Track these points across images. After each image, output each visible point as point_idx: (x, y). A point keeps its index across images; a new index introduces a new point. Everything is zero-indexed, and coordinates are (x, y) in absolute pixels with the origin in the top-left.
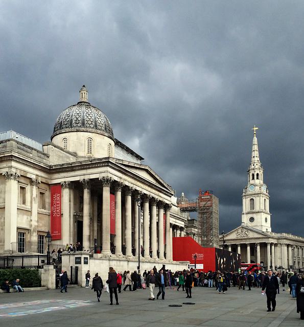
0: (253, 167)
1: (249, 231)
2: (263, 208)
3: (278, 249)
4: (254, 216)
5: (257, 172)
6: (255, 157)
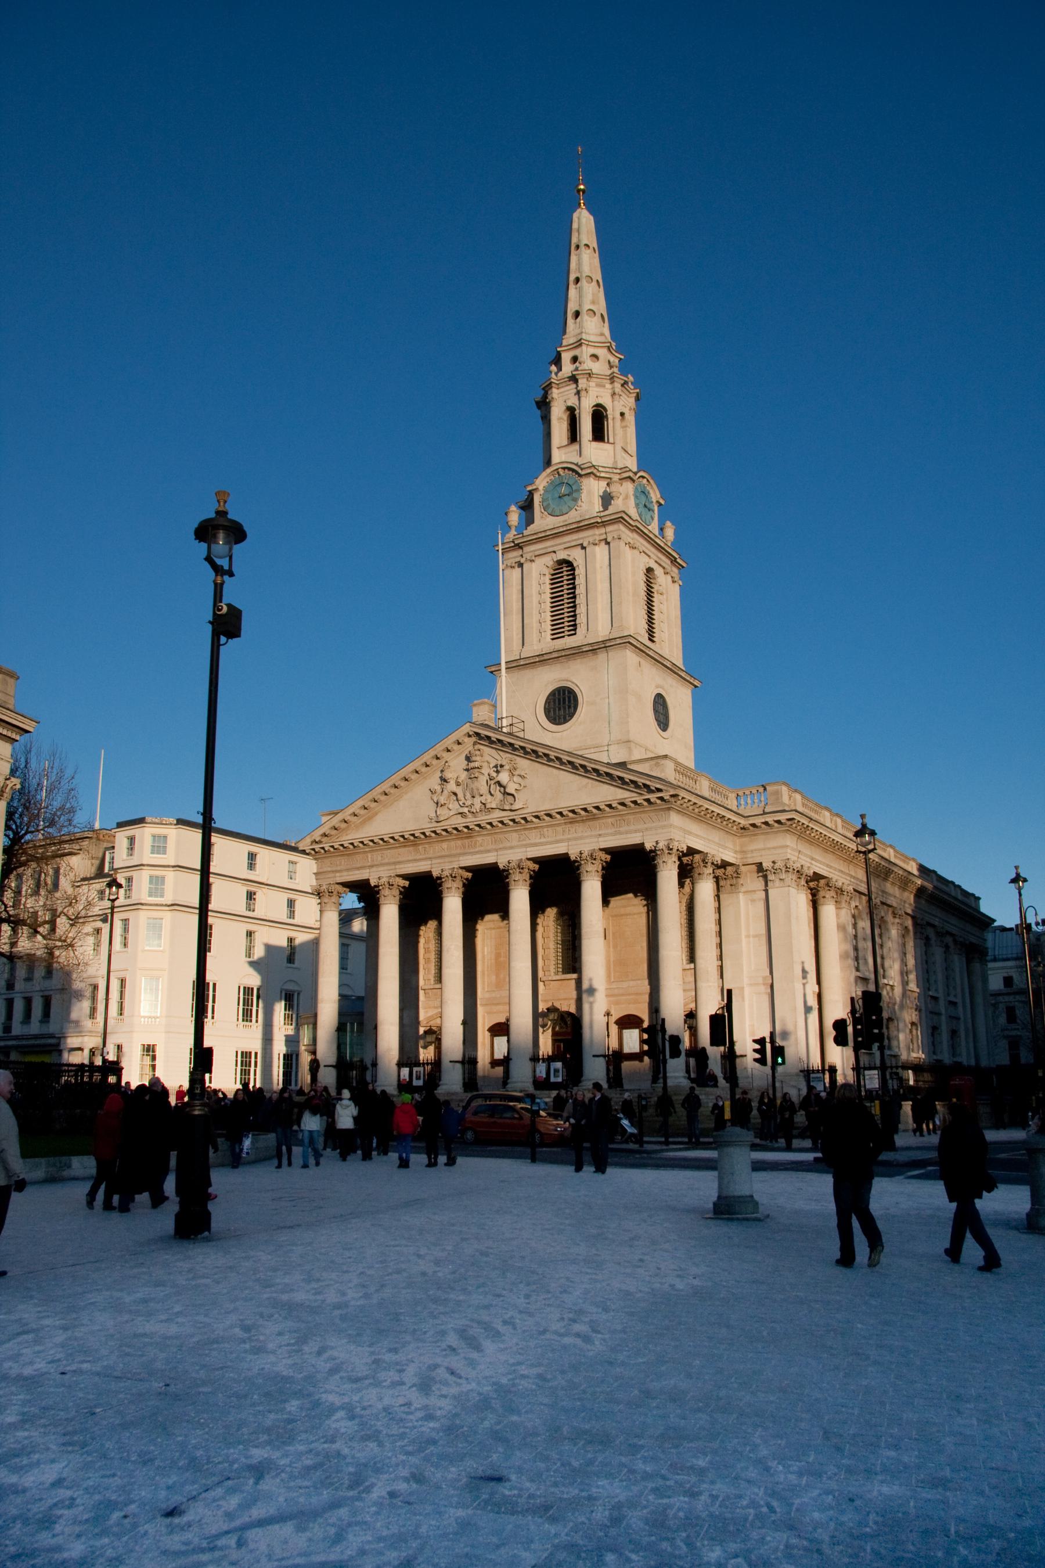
0: (567, 368)
1: (524, 764)
2: (635, 623)
3: (744, 907)
4: (576, 675)
5: (596, 394)
6: (584, 317)
